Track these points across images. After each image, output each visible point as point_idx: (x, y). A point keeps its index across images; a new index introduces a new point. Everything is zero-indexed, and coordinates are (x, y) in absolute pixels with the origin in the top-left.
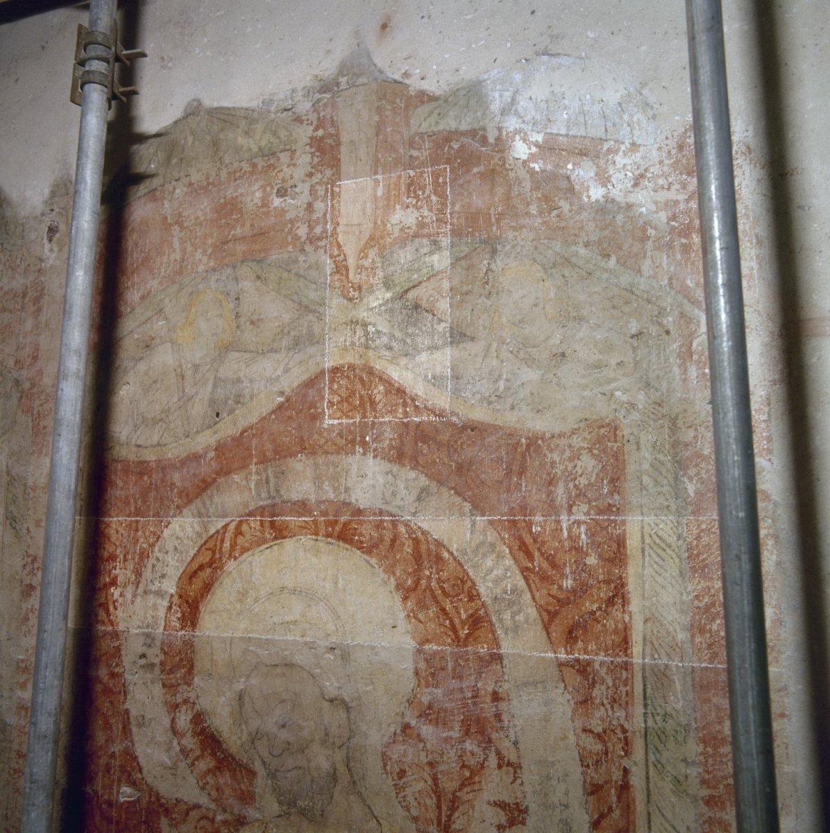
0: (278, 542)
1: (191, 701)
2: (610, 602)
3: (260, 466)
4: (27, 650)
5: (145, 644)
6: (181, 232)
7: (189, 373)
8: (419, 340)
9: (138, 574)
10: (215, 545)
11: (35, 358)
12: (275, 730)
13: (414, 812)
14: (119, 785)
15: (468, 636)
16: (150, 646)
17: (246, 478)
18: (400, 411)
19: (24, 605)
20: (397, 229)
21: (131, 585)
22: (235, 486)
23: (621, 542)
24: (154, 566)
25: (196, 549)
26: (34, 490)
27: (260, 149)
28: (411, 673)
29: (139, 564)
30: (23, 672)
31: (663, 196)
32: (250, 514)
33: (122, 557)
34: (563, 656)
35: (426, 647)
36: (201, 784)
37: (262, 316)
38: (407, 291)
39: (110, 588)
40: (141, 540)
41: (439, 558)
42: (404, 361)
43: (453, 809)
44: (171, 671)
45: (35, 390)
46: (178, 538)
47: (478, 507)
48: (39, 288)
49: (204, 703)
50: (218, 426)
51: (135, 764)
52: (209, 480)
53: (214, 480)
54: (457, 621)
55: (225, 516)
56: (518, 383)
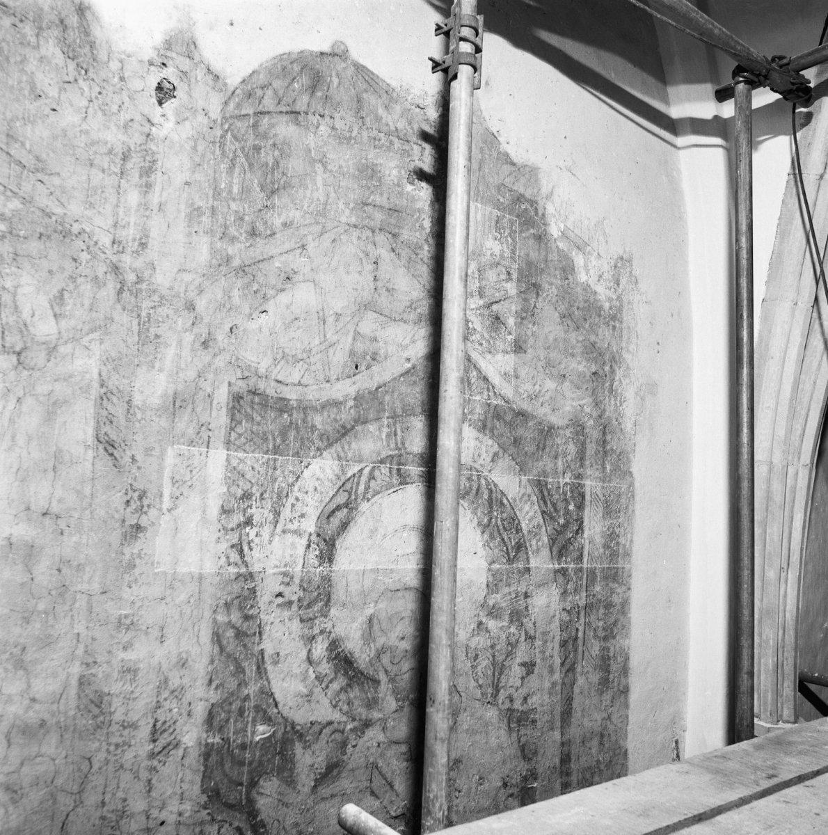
0: (402, 487)
1: (328, 630)
2: (577, 532)
3: (390, 420)
4: (133, 603)
5: (283, 583)
6: (325, 173)
7: (330, 320)
8: (497, 343)
9: (277, 514)
10: (352, 488)
11: (143, 245)
12: (397, 643)
13: (481, 682)
14: (254, 726)
15: (514, 556)
16: (288, 584)
17: (379, 429)
18: (486, 393)
19: (127, 551)
20: (489, 253)
21: (268, 524)
22: (369, 435)
23: (583, 497)
24: (293, 505)
25: (335, 490)
26: (144, 412)
27: (397, 130)
28: (484, 586)
29: (277, 503)
30: (128, 629)
31: (608, 293)
32: (382, 462)
33: (258, 495)
34: (557, 566)
35: (493, 566)
36: (334, 703)
37: (395, 287)
38: (492, 304)
39: (245, 528)
40: (280, 479)
41: (502, 504)
42: (489, 356)
43: (500, 674)
44: (309, 606)
45: (144, 286)
46: (318, 479)
47: (523, 470)
48: (148, 158)
49: (340, 631)
50: (357, 377)
51: (271, 700)
52: (349, 427)
53: (353, 427)
54: (510, 547)
55: (361, 461)
56: (545, 390)
